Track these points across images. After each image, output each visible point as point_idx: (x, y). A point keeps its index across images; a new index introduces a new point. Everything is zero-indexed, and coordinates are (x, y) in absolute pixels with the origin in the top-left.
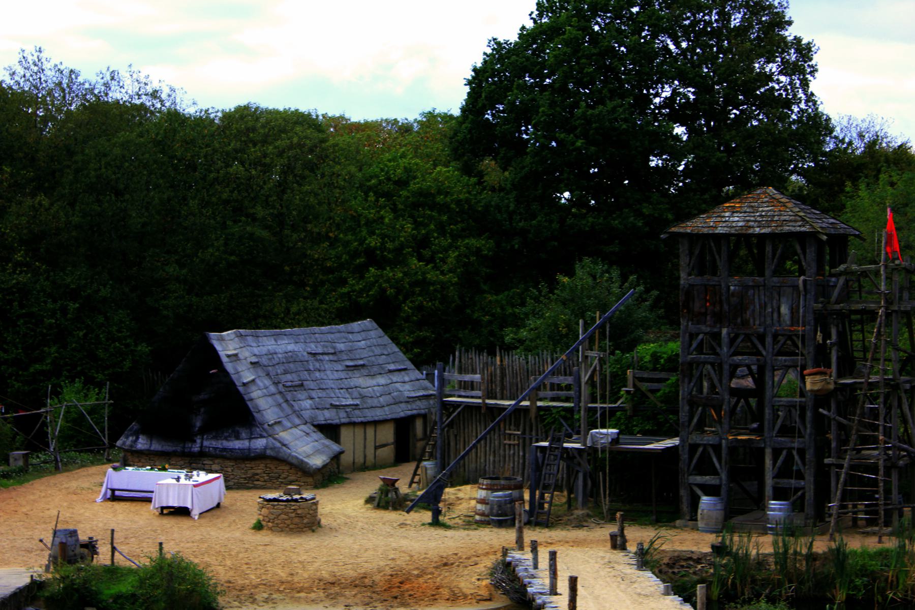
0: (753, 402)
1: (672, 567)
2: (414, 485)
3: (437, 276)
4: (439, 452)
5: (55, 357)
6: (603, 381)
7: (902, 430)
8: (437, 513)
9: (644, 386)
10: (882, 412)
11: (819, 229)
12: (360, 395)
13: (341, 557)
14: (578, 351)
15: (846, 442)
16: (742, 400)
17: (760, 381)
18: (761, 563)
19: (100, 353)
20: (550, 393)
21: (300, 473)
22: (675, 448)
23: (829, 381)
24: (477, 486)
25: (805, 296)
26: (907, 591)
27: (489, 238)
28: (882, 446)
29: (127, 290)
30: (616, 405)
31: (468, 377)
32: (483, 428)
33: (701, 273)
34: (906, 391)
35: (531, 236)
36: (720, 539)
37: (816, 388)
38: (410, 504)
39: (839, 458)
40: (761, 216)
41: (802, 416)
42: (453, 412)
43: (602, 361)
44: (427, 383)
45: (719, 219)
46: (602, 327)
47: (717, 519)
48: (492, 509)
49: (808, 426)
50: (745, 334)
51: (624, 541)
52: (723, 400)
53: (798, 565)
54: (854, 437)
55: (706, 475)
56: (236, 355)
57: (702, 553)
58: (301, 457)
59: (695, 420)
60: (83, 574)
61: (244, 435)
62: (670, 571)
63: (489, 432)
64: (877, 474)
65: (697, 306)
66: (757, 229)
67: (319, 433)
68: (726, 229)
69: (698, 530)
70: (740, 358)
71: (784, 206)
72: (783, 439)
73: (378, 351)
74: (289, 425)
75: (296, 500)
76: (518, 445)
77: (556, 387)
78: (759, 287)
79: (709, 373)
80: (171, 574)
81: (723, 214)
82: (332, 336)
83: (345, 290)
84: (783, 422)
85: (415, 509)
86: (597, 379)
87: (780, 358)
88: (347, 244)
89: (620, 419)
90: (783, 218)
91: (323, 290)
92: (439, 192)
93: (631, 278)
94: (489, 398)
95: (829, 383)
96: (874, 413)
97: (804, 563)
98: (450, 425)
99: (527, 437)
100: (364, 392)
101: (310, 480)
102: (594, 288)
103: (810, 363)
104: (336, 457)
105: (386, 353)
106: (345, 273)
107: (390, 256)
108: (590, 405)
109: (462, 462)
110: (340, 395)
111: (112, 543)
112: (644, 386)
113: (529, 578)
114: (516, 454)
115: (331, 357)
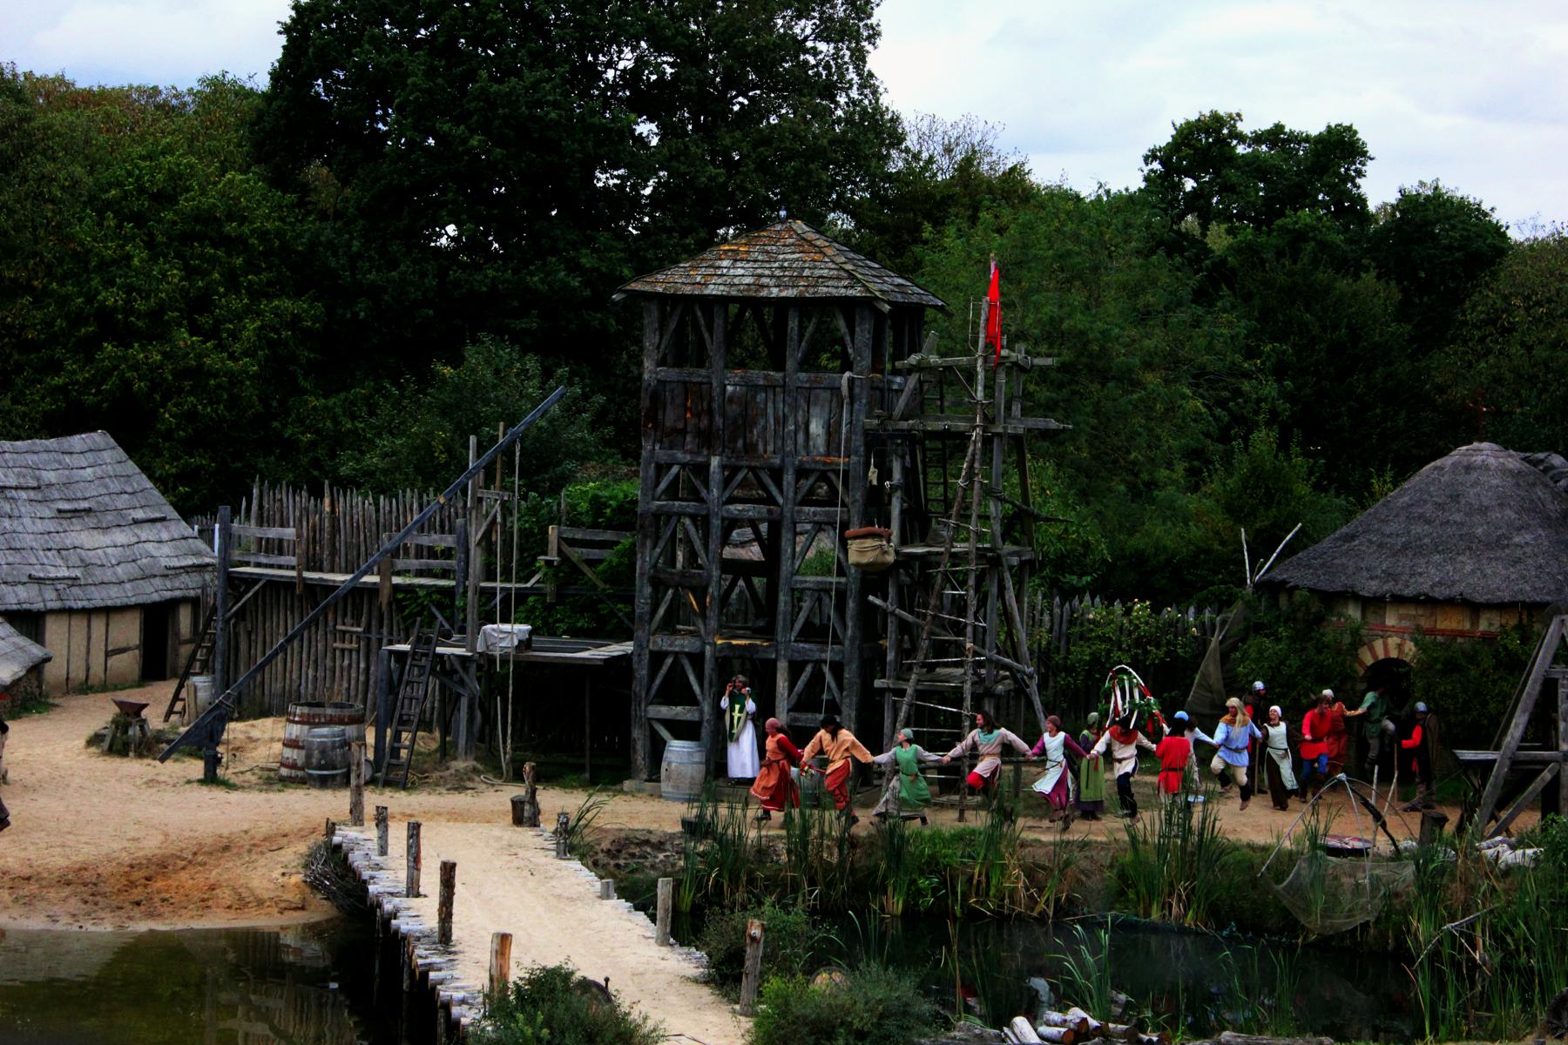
0: (758, 582)
1: (614, 857)
2: (173, 718)
4: (219, 660)
6: (507, 542)
7: (1002, 638)
8: (213, 762)
9: (576, 554)
10: (973, 604)
11: (878, 294)
12: (82, 561)
13: (43, 834)
14: (465, 493)
15: (911, 653)
16: (741, 583)
17: (771, 547)
18: (763, 852)
20: (414, 563)
22: (626, 658)
23: (886, 548)
24: (284, 719)
25: (852, 403)
26: (1002, 900)
27: (316, 299)
28: (970, 659)
30: (529, 585)
31: (273, 533)
32: (297, 620)
33: (680, 362)
34: (1011, 568)
35: (386, 297)
36: (695, 811)
37: (864, 560)
38: (165, 747)
39: (899, 678)
40: (782, 268)
41: (841, 608)
42: (246, 592)
43: (506, 509)
44: (201, 545)
45: (711, 271)
46: (508, 451)
47: (693, 778)
48: (309, 757)
49: (850, 624)
50: (752, 469)
51: (537, 812)
52: (710, 576)
53: (825, 855)
54: (925, 644)
55: (676, 705)
57: (665, 834)
59: (661, 611)
62: (612, 862)
63: (308, 626)
64: (960, 707)
65: (670, 418)
66: (775, 292)
67: (7, 626)
68: (722, 288)
69: (660, 797)
70: (740, 507)
71: (821, 252)
72: (807, 646)
73: (115, 486)
76: (358, 651)
77: (425, 553)
78: (774, 387)
79: (686, 532)
81: (718, 263)
82: (35, 457)
83: (58, 381)
84: (808, 617)
85: (174, 756)
86: (497, 538)
87: (806, 509)
88: (64, 300)
89: (533, 608)
90: (817, 272)
91: (19, 381)
92: (230, 217)
93: (560, 371)
95: (885, 553)
96: (960, 606)
97: (836, 851)
98: (241, 615)
99: (374, 636)
100: (90, 556)
102: (495, 387)
103: (855, 519)
104: (36, 669)
105: (129, 490)
106: (59, 352)
107: (140, 324)
108: (483, 584)
109: (259, 678)
110: (45, 561)
112: (576, 554)
113: (372, 869)
114: (354, 665)
115: (32, 494)
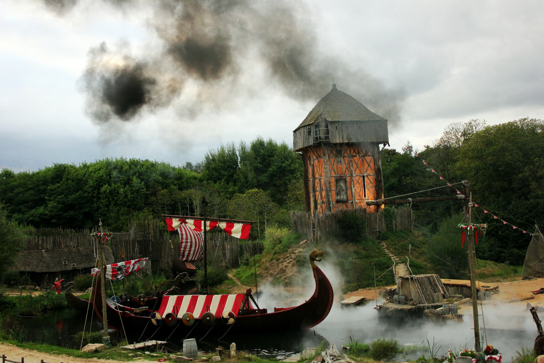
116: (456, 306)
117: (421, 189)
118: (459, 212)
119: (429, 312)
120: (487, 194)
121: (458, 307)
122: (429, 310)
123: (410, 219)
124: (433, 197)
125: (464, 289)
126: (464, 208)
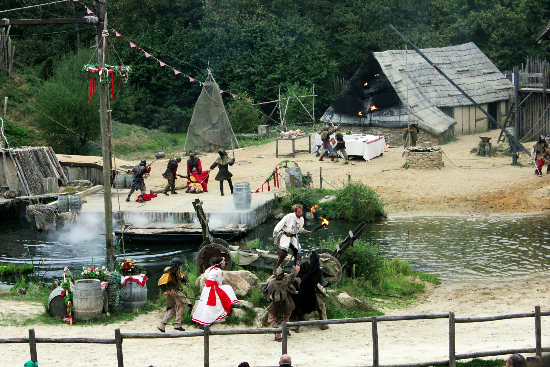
2: (501, 142)
3: (513, 15)
4: (516, 121)
5: (283, 70)
8: (516, 158)
19: (309, 67)
21: (430, 136)
29: (323, 29)
31: (534, 75)
42: (525, 96)
44: (507, 81)
56: (390, 65)
58: (431, 126)
60: (305, 193)
61: (396, 113)
73: (477, 62)
74: (423, 107)
75: (429, 151)
80: (355, 193)
82: (449, 53)
83: (455, 25)
91: (442, 26)
94: (548, 88)
98: (523, 105)
101: (436, 140)
104: (451, 127)
105: (482, 62)
106: (455, 15)
111: (321, 176)
115: (448, 66)
116: (80, 198)
117: (27, 3)
118: (89, 44)
119: (36, 209)
120: (135, 15)
121: (82, 199)
122: (34, 206)
123: (6, 53)
124: (47, 17)
125: (93, 170)
126: (97, 38)
